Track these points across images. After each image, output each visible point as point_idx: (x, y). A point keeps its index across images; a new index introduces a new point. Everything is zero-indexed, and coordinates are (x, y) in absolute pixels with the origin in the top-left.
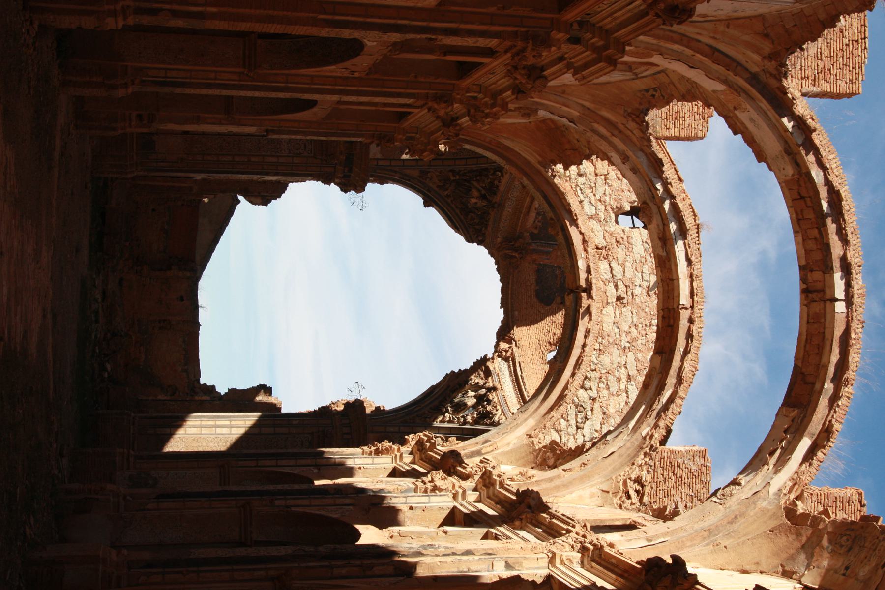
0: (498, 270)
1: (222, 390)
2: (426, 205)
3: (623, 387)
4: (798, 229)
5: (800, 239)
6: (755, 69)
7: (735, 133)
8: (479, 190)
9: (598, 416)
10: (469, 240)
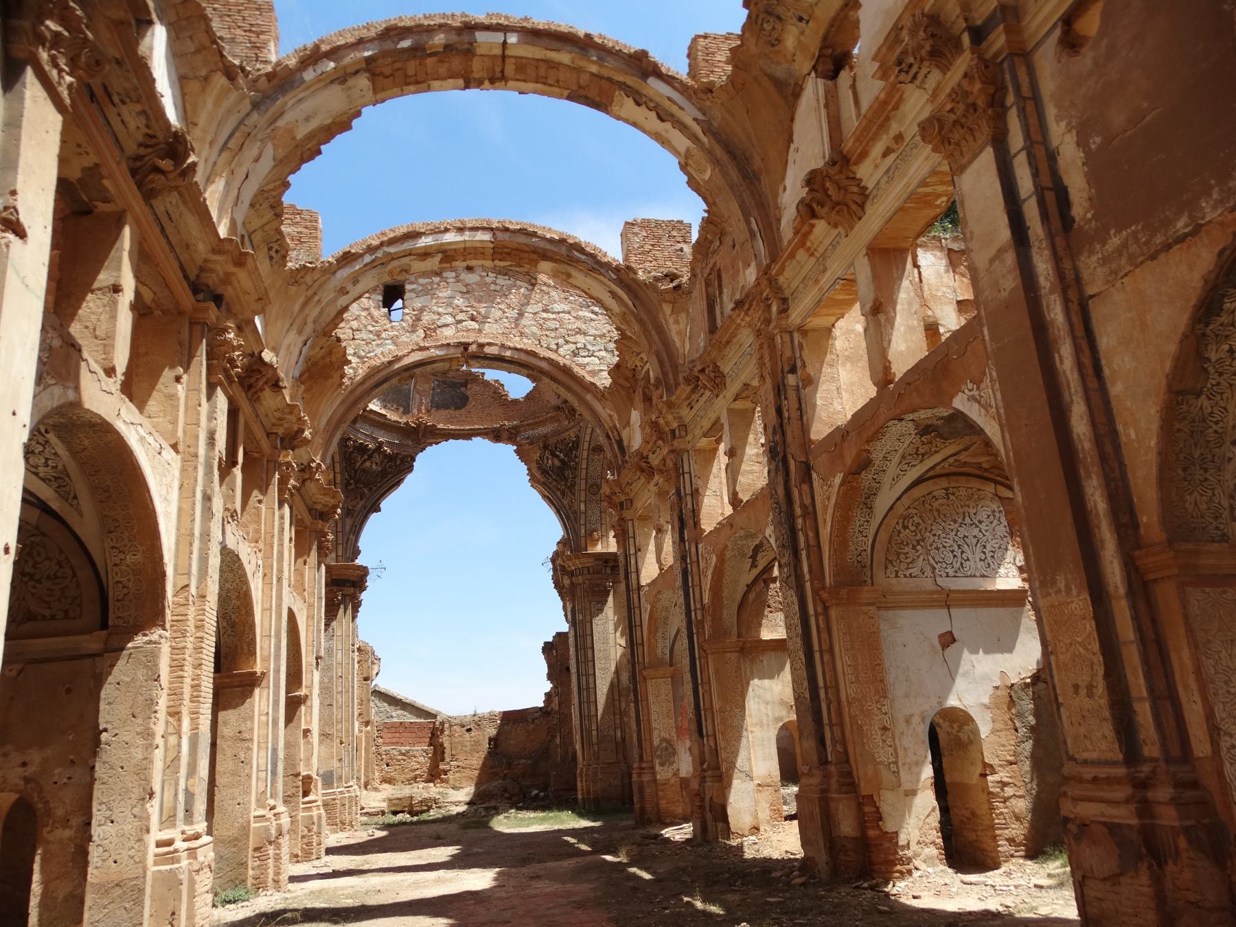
0: (437, 443)
1: (548, 686)
2: (378, 510)
3: (554, 316)
4: (425, 85)
5: (436, 84)
6: (246, 106)
7: (319, 152)
8: (364, 462)
9: (581, 339)
10: (410, 469)
